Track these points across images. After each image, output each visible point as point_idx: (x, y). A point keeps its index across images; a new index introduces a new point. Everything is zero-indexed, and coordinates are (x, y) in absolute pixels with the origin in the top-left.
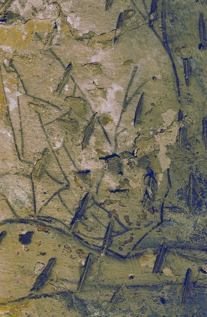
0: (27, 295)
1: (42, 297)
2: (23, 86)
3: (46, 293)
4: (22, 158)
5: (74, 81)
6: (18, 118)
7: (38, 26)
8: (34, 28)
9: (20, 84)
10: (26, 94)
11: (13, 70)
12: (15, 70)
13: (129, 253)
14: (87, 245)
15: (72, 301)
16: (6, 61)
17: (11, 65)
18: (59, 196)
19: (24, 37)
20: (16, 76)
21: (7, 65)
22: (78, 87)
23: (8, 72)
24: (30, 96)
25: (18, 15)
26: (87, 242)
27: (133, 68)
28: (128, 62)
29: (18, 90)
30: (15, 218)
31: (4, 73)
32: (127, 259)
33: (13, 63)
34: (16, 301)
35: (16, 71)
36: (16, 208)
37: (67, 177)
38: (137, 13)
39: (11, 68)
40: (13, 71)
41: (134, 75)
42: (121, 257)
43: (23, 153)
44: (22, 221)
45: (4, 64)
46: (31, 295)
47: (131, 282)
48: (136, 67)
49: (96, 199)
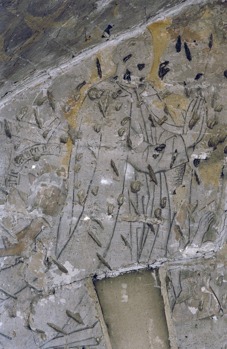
2: (7, 268)
5: (7, 299)
7: (42, 280)
8: (41, 277)
9: (8, 266)
11: (17, 263)
16: (22, 259)
17: (20, 262)
19: (36, 271)
20: (13, 264)
21: (20, 259)
22: (2, 301)
23: (16, 260)
25: (49, 268)
27: (11, 337)
28: (14, 334)
29: (5, 264)
31: (16, 257)
33: (21, 263)
35: (16, 264)
38: (44, 343)
39: (18, 261)
40: (16, 262)
41: (7, 337)
45: (21, 257)
48: (11, 339)
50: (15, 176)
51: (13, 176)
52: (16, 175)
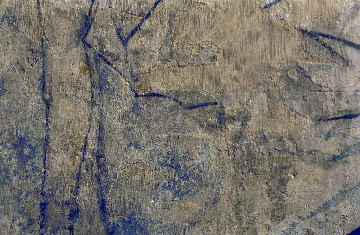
13: (90, 47)
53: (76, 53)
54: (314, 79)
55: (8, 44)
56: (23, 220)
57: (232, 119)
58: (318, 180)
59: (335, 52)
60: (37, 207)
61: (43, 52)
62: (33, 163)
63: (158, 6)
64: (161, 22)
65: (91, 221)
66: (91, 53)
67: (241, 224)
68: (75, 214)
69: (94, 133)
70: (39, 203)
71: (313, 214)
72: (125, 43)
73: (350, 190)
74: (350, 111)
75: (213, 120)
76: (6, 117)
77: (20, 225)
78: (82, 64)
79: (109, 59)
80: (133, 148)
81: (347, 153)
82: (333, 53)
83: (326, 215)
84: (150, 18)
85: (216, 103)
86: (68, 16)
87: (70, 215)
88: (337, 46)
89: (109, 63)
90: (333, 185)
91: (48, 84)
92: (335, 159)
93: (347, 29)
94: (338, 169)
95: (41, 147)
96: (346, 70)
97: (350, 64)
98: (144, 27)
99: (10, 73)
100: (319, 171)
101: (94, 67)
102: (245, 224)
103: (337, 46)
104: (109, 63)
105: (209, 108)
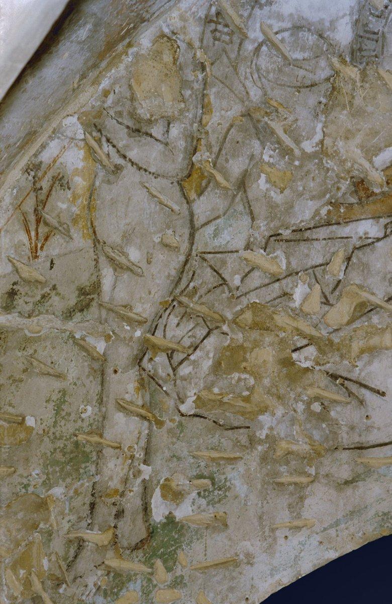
0: (99, 238)
1: (96, 257)
3: (100, 261)
4: (272, 239)
6: (323, 237)
10: (355, 248)
11: (388, 233)
12: (388, 236)
13: (144, 370)
14: (158, 317)
15: (88, 294)
18: (221, 285)
24: (353, 252)
26: (161, 317)
30: (197, 226)
32: (137, 367)
34: (92, 223)
35: (386, 236)
36: (210, 229)
37: (246, 296)
40: (385, 233)
42: (141, 360)
43: (278, 241)
44: (192, 236)
46: (99, 242)
47: (110, 371)
49: (215, 331)
50: (373, 40)
51: (368, 39)
52: (375, 37)
53: (133, 373)
54: (333, 413)
55: (72, 361)
56: (73, 518)
57: (261, 442)
58: (330, 500)
59: (352, 393)
60: (87, 507)
61: (103, 371)
62: (86, 467)
63: (205, 341)
64: (207, 354)
65: (134, 521)
66: (145, 376)
67: (264, 533)
68: (119, 514)
69: (143, 443)
70: (89, 502)
71: (325, 529)
72: (174, 370)
73: (359, 511)
74: (362, 444)
75: (244, 440)
76: (65, 425)
77: (69, 521)
78: (136, 384)
79: (161, 382)
80: (175, 459)
81: (357, 479)
82: (350, 394)
83: (337, 531)
84: (198, 351)
85: (248, 427)
86: (127, 342)
87: (115, 515)
88: (354, 388)
89: (160, 386)
90: (344, 505)
91: (105, 399)
92: (347, 483)
93: (363, 374)
94: (349, 491)
95: (94, 453)
96: (360, 409)
97: (364, 403)
98: (192, 357)
99: (71, 387)
100: (333, 492)
101: (147, 388)
102: (267, 534)
103: (354, 388)
104: (160, 386)
105: (242, 431)
